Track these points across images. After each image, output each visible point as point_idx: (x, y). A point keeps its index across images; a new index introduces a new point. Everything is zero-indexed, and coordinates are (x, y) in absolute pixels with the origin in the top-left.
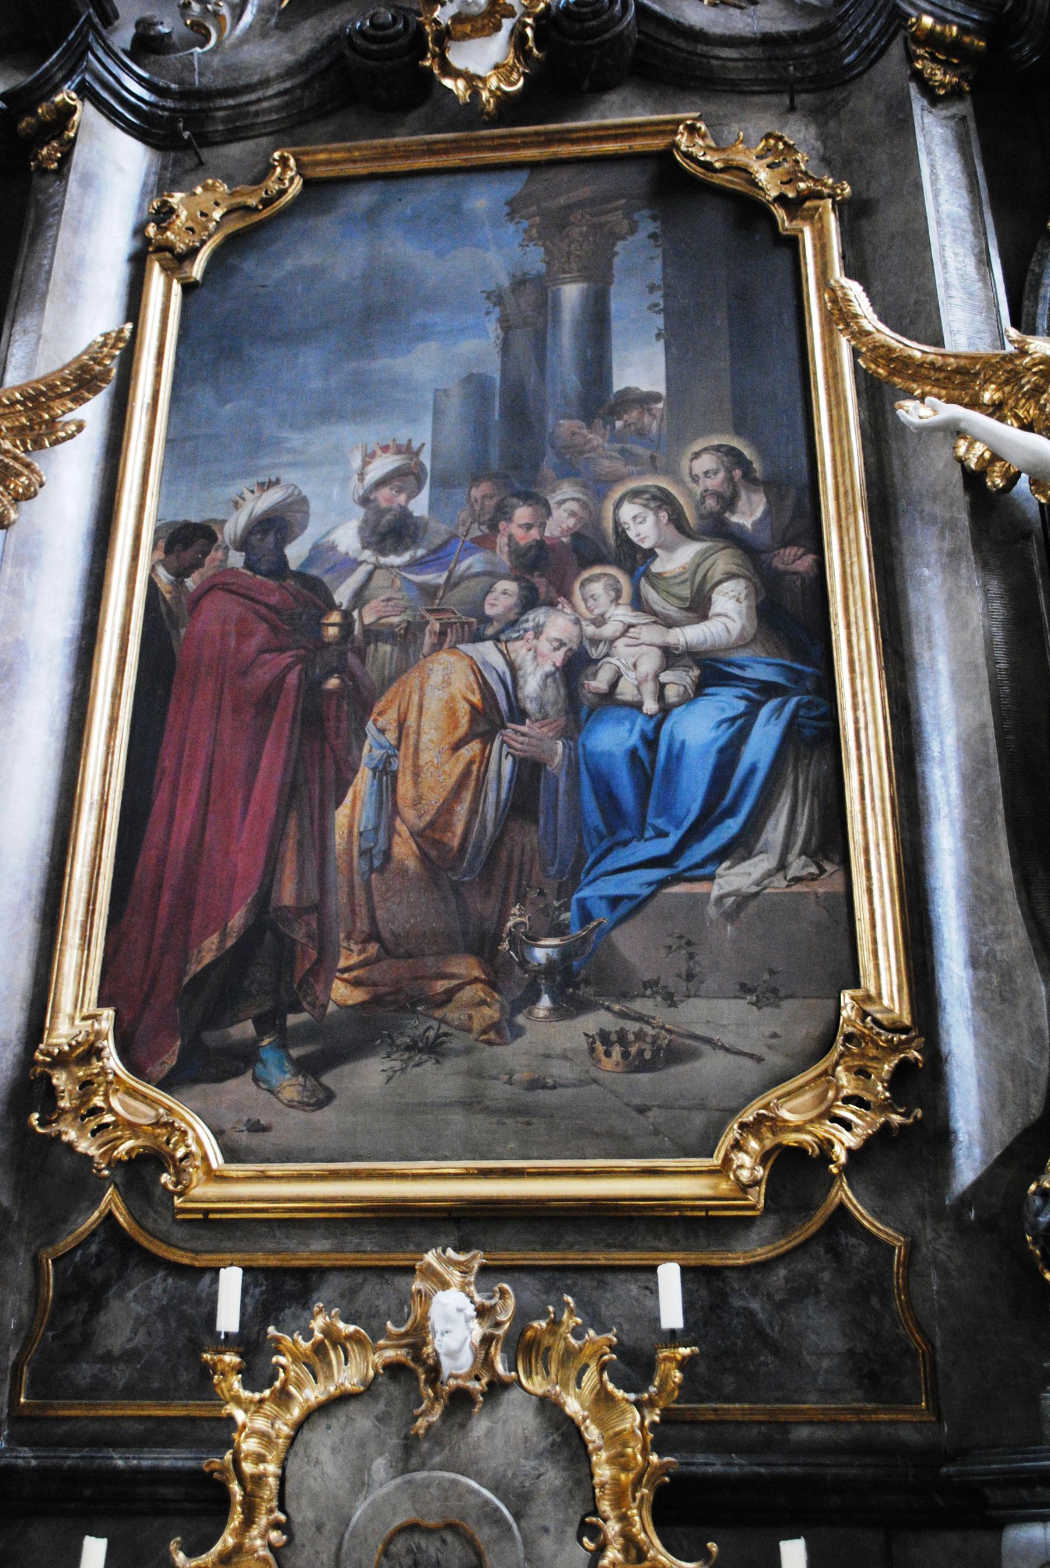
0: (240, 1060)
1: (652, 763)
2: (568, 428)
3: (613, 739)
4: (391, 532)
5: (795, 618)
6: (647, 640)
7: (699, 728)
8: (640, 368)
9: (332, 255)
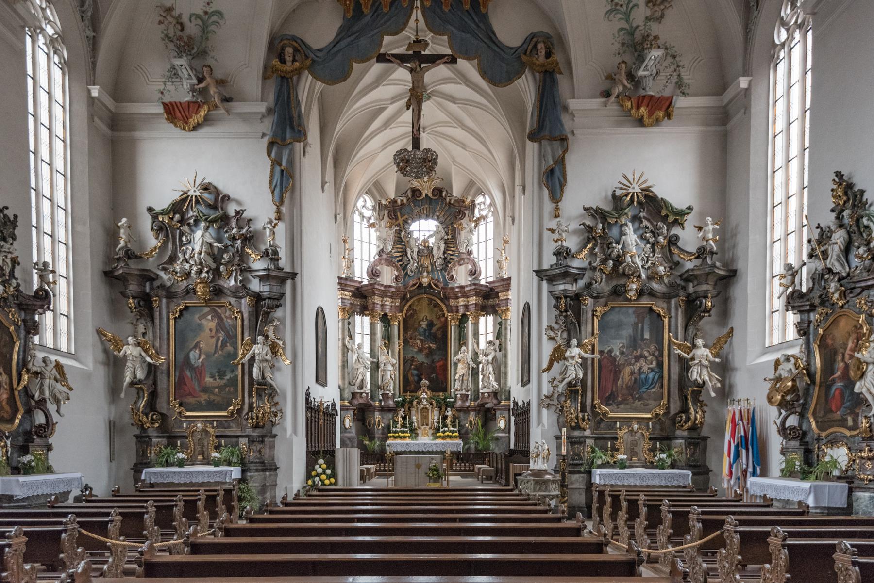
0: (611, 404)
1: (646, 379)
2: (640, 342)
3: (643, 376)
4: (622, 353)
5: (660, 365)
6: (646, 366)
7: (651, 376)
8: (647, 336)
9: (614, 317)
